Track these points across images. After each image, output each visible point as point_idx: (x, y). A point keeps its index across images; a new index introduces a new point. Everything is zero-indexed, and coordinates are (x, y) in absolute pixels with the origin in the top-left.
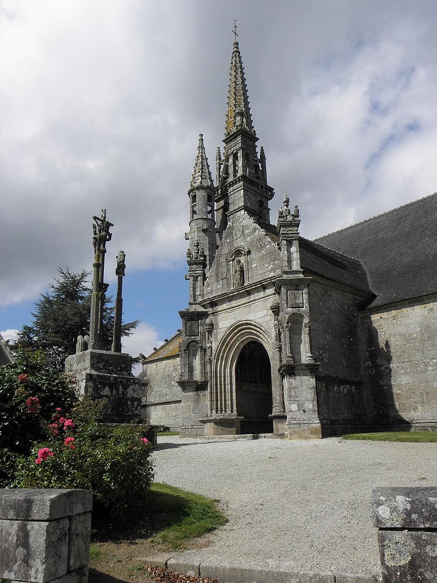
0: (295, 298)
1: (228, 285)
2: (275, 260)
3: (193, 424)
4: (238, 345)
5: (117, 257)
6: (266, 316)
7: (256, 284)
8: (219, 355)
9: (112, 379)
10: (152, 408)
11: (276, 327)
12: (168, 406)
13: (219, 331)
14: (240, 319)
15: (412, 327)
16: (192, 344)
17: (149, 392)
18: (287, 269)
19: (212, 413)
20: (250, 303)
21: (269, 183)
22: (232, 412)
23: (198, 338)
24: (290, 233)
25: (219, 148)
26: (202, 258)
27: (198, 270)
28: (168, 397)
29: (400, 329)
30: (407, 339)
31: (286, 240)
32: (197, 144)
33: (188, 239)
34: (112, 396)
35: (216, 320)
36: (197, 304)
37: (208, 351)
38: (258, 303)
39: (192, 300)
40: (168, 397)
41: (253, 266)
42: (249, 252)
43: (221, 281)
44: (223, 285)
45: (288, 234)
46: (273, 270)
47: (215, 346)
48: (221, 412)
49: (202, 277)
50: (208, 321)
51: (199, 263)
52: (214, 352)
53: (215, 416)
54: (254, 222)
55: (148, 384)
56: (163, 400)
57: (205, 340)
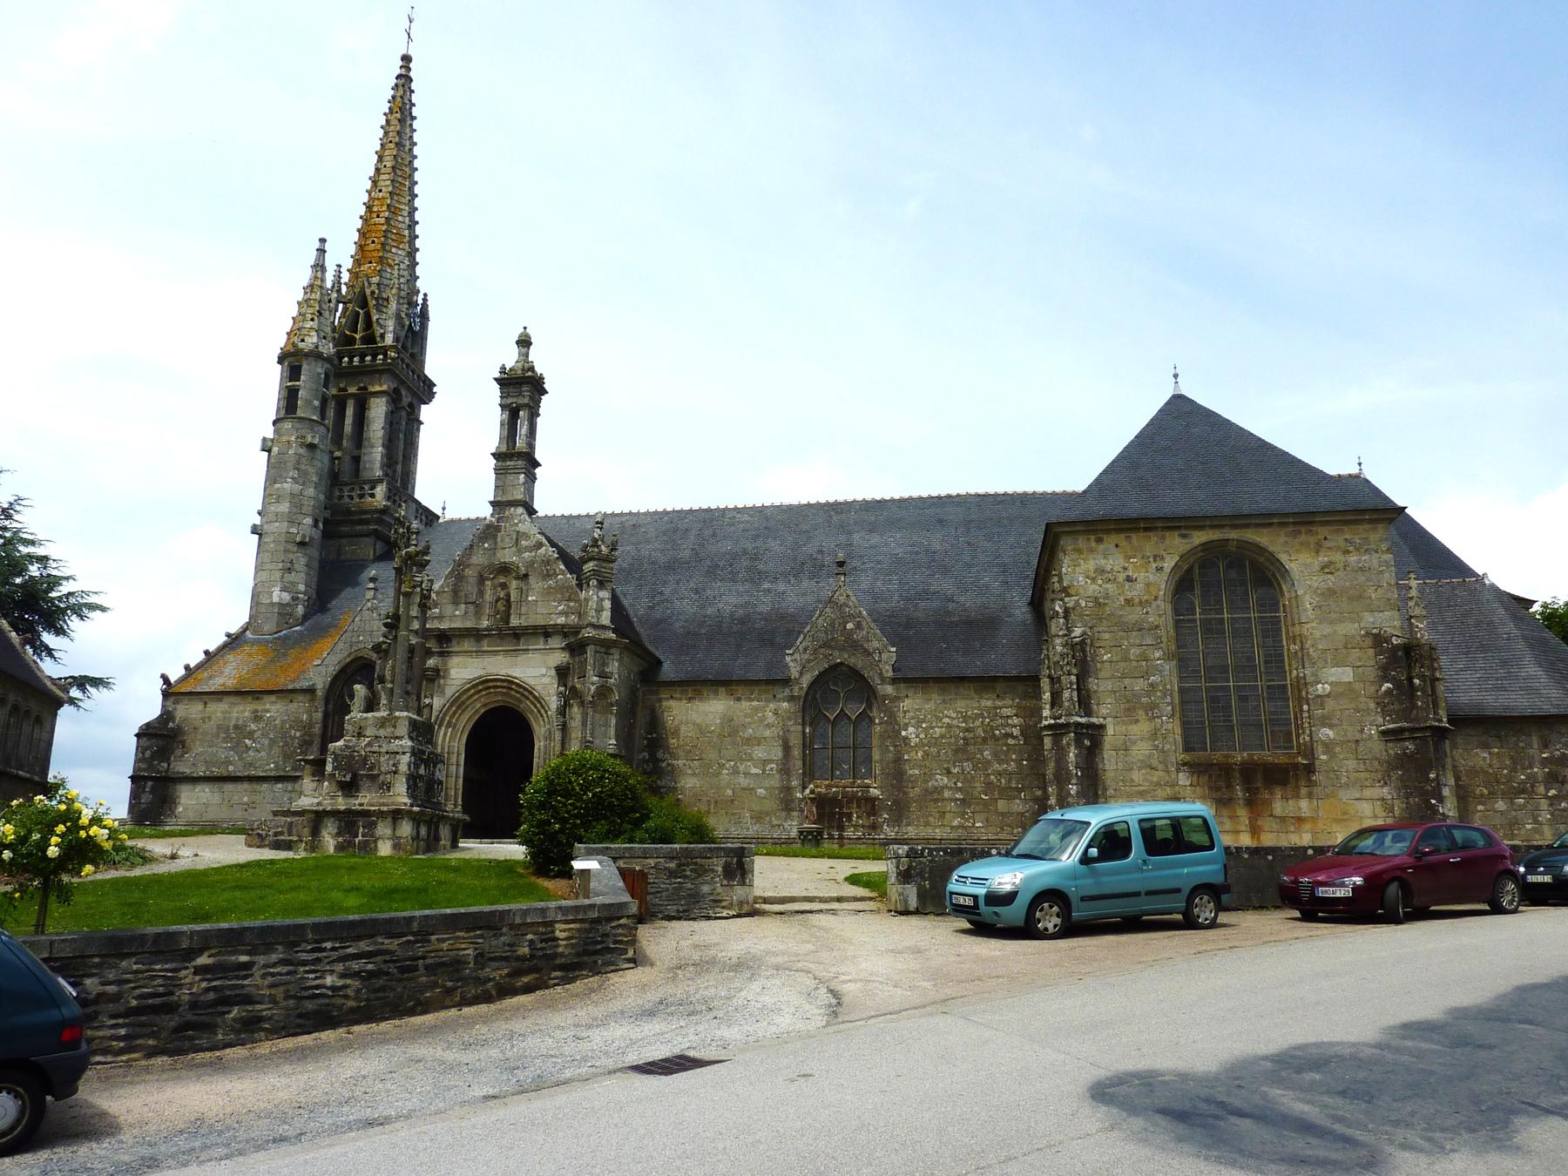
0: (604, 664)
1: (478, 614)
2: (569, 600)
4: (477, 708)
7: (535, 627)
12: (229, 787)
14: (494, 671)
15: (711, 717)
17: (178, 752)
18: (594, 620)
21: (430, 371)
28: (231, 768)
29: (695, 716)
30: (702, 730)
32: (312, 257)
33: (269, 451)
40: (231, 768)
46: (565, 614)
47: (437, 703)
50: (431, 662)
55: (175, 736)
56: (216, 771)
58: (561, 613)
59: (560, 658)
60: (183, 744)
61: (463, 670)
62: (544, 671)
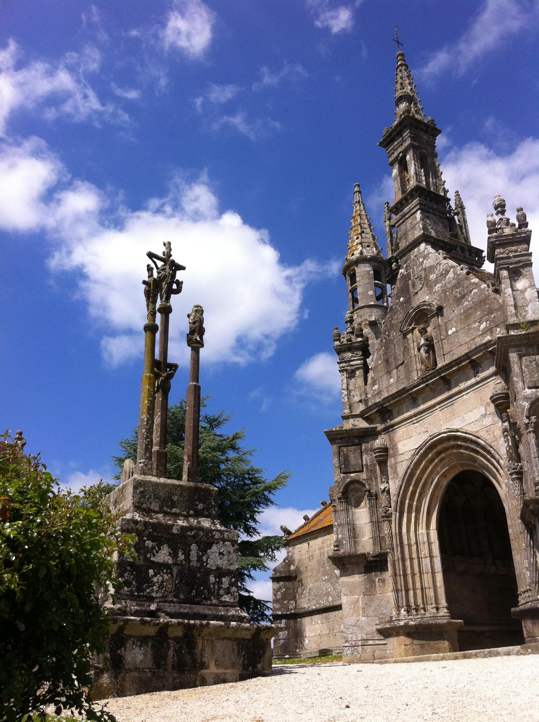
1: (408, 373)
2: (490, 312)
3: (365, 637)
4: (437, 480)
5: (189, 316)
6: (484, 416)
8: (403, 503)
9: (175, 531)
10: (306, 620)
11: (506, 433)
13: (400, 458)
14: (435, 431)
16: (352, 487)
17: (300, 590)
19: (399, 614)
20: (451, 400)
22: (437, 609)
23: (363, 476)
24: (515, 257)
25: (388, 203)
26: (360, 339)
27: (354, 360)
31: (507, 269)
34: (175, 564)
35: (392, 440)
36: (356, 416)
37: (383, 498)
38: (465, 397)
39: (347, 411)
41: (450, 332)
42: (440, 310)
43: (395, 371)
44: (398, 377)
45: (509, 258)
46: (490, 330)
47: (394, 486)
48: (417, 610)
49: (361, 371)
51: (357, 349)
52: (393, 498)
53: (404, 618)
54: (445, 258)
55: (296, 577)
57: (376, 478)
58: (484, 333)
59: (495, 385)
60: (301, 581)
61: (409, 439)
62: (482, 410)
